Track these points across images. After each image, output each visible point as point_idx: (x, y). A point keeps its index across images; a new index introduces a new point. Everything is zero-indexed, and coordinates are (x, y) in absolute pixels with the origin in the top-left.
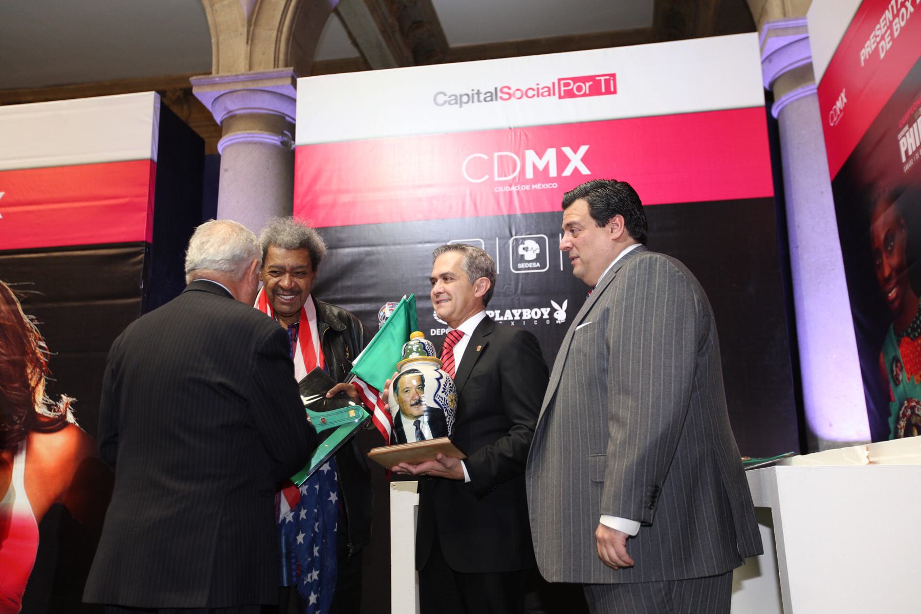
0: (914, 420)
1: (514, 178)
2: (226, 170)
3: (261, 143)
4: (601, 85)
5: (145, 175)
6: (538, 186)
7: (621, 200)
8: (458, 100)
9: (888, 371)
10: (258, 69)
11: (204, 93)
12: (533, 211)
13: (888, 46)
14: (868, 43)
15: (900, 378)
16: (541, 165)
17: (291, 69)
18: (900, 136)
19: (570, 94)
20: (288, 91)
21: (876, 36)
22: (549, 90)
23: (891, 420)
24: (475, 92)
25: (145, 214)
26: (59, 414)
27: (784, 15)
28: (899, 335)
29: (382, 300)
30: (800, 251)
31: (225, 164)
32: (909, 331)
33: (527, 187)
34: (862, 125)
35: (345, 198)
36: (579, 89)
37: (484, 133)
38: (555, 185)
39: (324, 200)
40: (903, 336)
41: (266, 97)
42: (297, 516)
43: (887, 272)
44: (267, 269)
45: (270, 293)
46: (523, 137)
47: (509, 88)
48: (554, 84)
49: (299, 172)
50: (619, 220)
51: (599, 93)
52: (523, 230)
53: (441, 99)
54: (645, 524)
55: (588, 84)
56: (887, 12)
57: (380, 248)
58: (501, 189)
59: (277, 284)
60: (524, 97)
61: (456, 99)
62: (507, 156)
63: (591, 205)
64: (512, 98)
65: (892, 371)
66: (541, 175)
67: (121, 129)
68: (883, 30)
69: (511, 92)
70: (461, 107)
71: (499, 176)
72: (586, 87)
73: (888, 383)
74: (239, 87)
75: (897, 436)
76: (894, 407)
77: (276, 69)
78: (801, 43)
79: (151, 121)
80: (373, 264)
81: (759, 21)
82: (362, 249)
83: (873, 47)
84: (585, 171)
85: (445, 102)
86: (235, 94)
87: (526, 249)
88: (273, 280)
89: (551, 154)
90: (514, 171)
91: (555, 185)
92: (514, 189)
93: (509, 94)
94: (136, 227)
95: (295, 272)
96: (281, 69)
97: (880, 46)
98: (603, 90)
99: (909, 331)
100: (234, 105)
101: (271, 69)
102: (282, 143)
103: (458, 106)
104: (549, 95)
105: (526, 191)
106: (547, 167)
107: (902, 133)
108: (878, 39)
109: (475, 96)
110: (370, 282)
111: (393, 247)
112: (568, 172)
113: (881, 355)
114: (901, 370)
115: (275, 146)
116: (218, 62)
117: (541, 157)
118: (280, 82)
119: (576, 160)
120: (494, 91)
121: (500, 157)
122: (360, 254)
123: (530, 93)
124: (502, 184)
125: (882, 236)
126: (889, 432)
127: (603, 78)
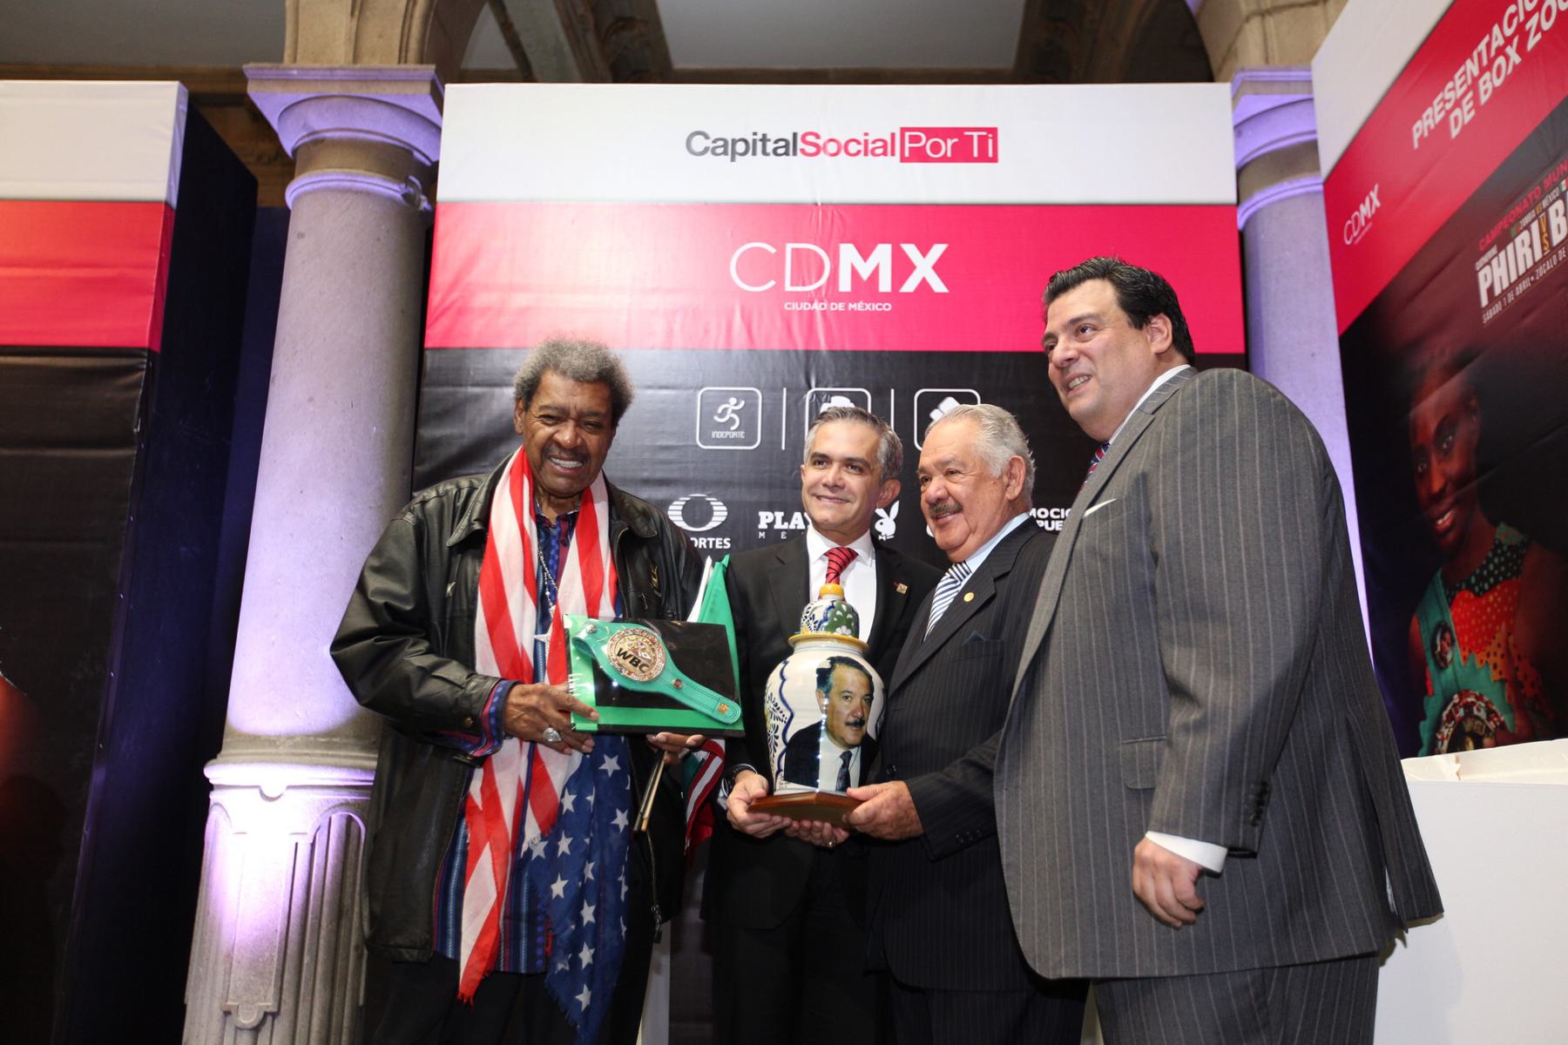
0: (1468, 726)
1: (819, 289)
2: (301, 236)
3: (368, 194)
4: (972, 146)
6: (858, 306)
8: (728, 148)
9: (1426, 645)
10: (369, 62)
11: (269, 99)
12: (848, 347)
13: (1468, 118)
14: (1429, 111)
15: (1449, 657)
16: (865, 273)
17: (430, 69)
18: (1479, 264)
19: (918, 156)
20: (426, 107)
21: (1446, 101)
22: (885, 147)
23: (1425, 728)
24: (759, 136)
25: (152, 299)
27: (1267, 61)
28: (1452, 590)
31: (296, 225)
32: (1473, 580)
33: (840, 306)
34: (1403, 246)
35: (520, 300)
36: (936, 148)
38: (887, 307)
39: (481, 300)
40: (1460, 589)
42: (552, 849)
43: (1437, 485)
46: (837, 220)
47: (818, 136)
48: (893, 135)
51: (969, 158)
52: (830, 377)
53: (699, 143)
55: (950, 142)
56: (1468, 62)
58: (795, 306)
61: (725, 146)
65: (1434, 646)
66: (865, 287)
67: (114, 143)
68: (1460, 92)
69: (821, 142)
70: (733, 159)
71: (792, 285)
72: (947, 146)
73: (1426, 665)
74: (335, 90)
75: (1433, 751)
76: (1432, 705)
77: (403, 66)
78: (1299, 107)
79: (169, 133)
81: (1220, 70)
83: (1439, 118)
84: (938, 286)
85: (706, 150)
86: (327, 102)
89: (883, 254)
90: (819, 278)
91: (887, 307)
92: (817, 306)
93: (816, 145)
94: (131, 322)
96: (411, 66)
97: (1452, 117)
98: (976, 154)
99: (1473, 580)
100: (323, 121)
101: (395, 65)
102: (404, 196)
104: (885, 154)
106: (875, 274)
107: (1484, 259)
108: (1448, 106)
109: (758, 144)
112: (910, 286)
113: (1415, 619)
114: (1452, 643)
115: (391, 199)
116: (296, 42)
117: (865, 257)
118: (409, 89)
119: (925, 267)
120: (791, 139)
121: (795, 251)
124: (799, 297)
125: (1433, 427)
126: (1420, 745)
127: (975, 134)
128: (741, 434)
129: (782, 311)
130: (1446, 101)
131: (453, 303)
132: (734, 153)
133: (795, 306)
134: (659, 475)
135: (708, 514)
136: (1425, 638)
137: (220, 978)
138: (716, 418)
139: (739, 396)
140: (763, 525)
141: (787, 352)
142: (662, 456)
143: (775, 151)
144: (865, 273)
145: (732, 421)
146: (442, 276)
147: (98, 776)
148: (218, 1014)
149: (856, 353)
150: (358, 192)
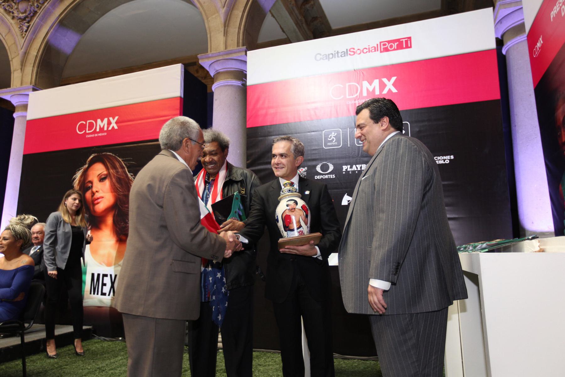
2: (216, 100)
3: (232, 85)
4: (403, 44)
7: (387, 109)
10: (230, 48)
11: (205, 63)
14: (555, 7)
16: (371, 89)
17: (245, 47)
19: (386, 50)
21: (559, 3)
30: (517, 128)
31: (215, 97)
34: (552, 55)
35: (272, 111)
36: (391, 47)
37: (340, 73)
39: (262, 112)
41: (234, 62)
46: (361, 74)
50: (386, 120)
51: (402, 48)
53: (319, 57)
54: (393, 284)
55: (396, 44)
58: (350, 103)
60: (362, 54)
63: (371, 112)
64: (356, 55)
67: (168, 82)
69: (355, 51)
71: (349, 96)
72: (395, 45)
74: (221, 58)
78: (519, 11)
79: (179, 78)
83: (558, 10)
84: (394, 90)
85: (321, 59)
86: (219, 62)
89: (376, 83)
90: (357, 92)
93: (354, 52)
96: (240, 47)
98: (404, 46)
100: (219, 67)
101: (236, 48)
102: (242, 84)
106: (374, 89)
108: (561, 5)
109: (336, 54)
115: (239, 86)
116: (211, 46)
118: (239, 54)
121: (350, 86)
123: (365, 51)
124: (351, 99)
127: (404, 40)
128: (336, 143)
130: (559, 3)
133: (350, 103)
134: (313, 157)
135: (328, 168)
139: (335, 132)
140: (344, 170)
142: (314, 152)
145: (333, 139)
146: (250, 107)
150: (229, 86)
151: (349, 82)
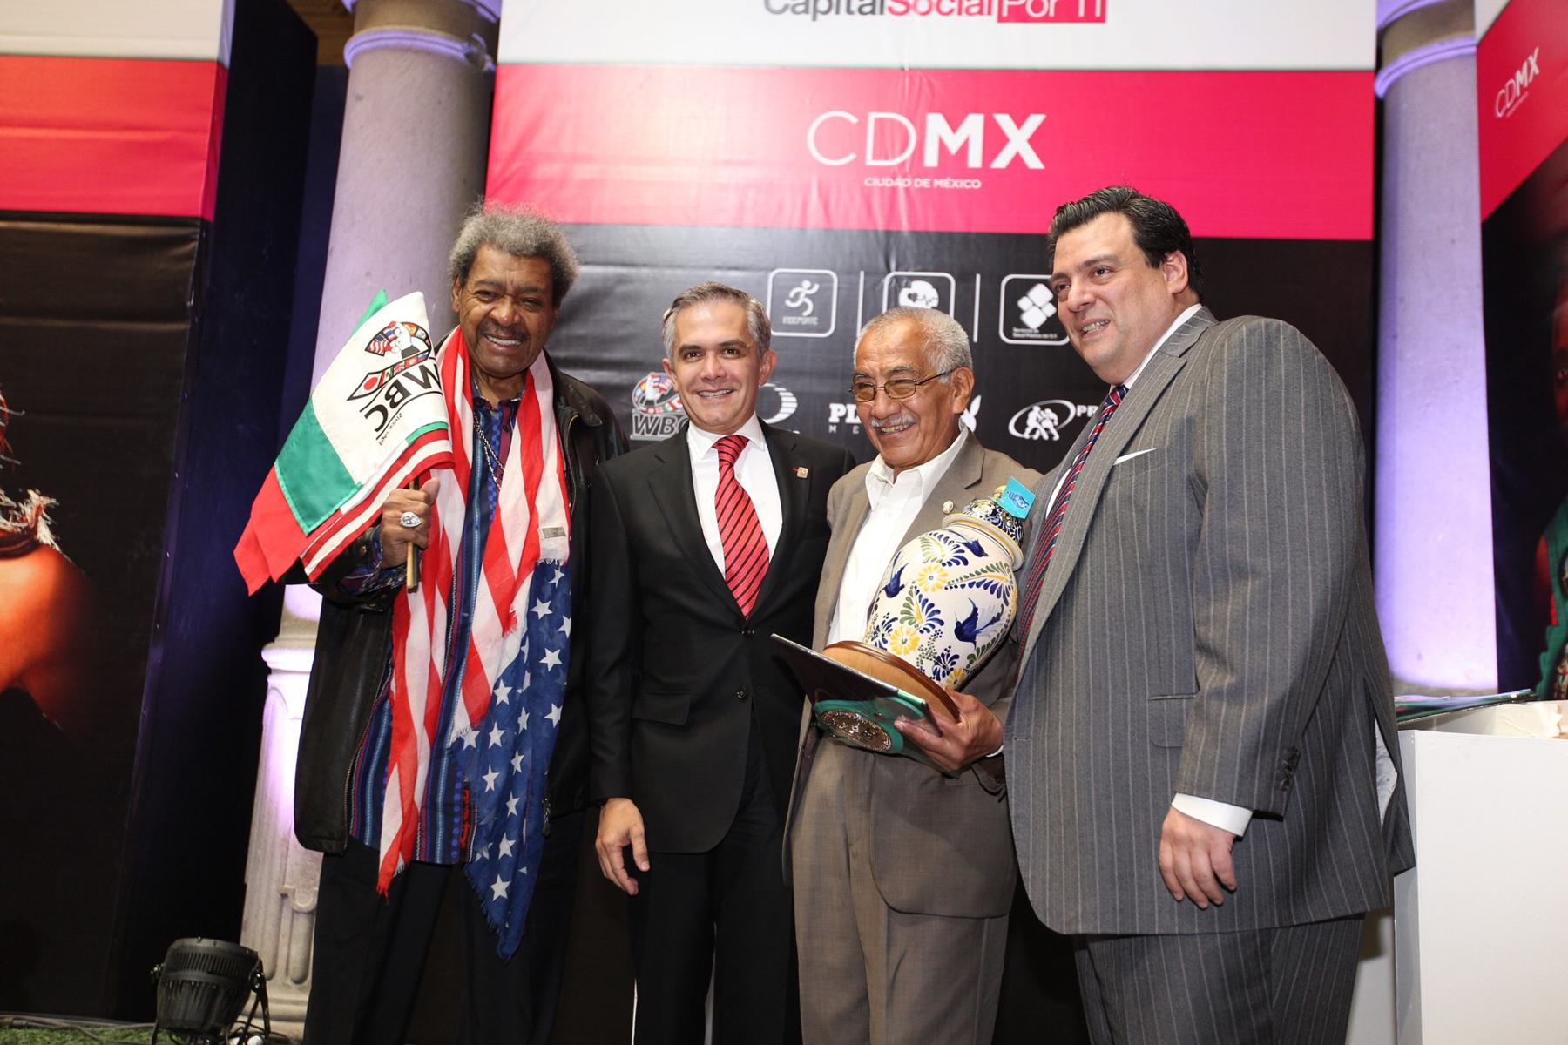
1: (903, 163)
2: (359, 98)
5: (207, 91)
6: (944, 183)
12: (932, 227)
16: (953, 148)
25: (203, 165)
26: (24, 525)
29: (642, 367)
31: (355, 87)
33: (925, 183)
35: (583, 172)
38: (976, 184)
39: (544, 171)
44: (471, 287)
45: (471, 331)
46: (926, 88)
49: (502, 114)
57: (645, 271)
58: (876, 182)
59: (487, 315)
60: (934, 13)
62: (893, 121)
64: (912, 13)
66: (953, 162)
70: (814, 19)
71: (875, 157)
80: (627, 299)
82: (611, 270)
84: (1033, 162)
87: (913, 297)
88: (480, 308)
89: (974, 125)
91: (976, 184)
92: (900, 183)
94: (185, 189)
95: (518, 297)
98: (1081, 13)
102: (468, 56)
103: (809, 16)
104: (981, 12)
105: (922, 190)
106: (964, 149)
110: (622, 332)
111: (668, 272)
112: (1002, 161)
115: (453, 59)
119: (1019, 140)
121: (879, 122)
122: (606, 279)
124: (881, 172)
128: (814, 321)
129: (863, 188)
131: (514, 174)
132: (816, 11)
133: (876, 182)
136: (1553, 563)
137: (277, 861)
138: (788, 303)
139: (814, 279)
140: (834, 418)
141: (865, 233)
143: (860, 11)
144: (953, 148)
145: (804, 306)
146: (502, 145)
147: (155, 655)
148: (275, 896)
149: (940, 235)
151: (880, 110)
